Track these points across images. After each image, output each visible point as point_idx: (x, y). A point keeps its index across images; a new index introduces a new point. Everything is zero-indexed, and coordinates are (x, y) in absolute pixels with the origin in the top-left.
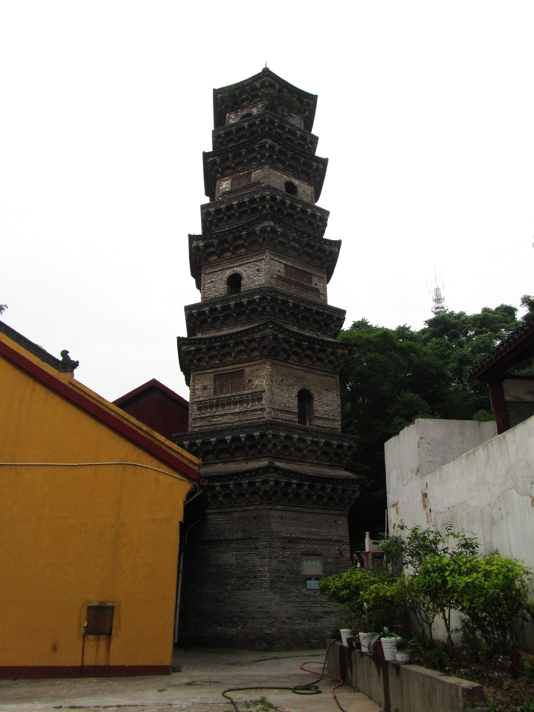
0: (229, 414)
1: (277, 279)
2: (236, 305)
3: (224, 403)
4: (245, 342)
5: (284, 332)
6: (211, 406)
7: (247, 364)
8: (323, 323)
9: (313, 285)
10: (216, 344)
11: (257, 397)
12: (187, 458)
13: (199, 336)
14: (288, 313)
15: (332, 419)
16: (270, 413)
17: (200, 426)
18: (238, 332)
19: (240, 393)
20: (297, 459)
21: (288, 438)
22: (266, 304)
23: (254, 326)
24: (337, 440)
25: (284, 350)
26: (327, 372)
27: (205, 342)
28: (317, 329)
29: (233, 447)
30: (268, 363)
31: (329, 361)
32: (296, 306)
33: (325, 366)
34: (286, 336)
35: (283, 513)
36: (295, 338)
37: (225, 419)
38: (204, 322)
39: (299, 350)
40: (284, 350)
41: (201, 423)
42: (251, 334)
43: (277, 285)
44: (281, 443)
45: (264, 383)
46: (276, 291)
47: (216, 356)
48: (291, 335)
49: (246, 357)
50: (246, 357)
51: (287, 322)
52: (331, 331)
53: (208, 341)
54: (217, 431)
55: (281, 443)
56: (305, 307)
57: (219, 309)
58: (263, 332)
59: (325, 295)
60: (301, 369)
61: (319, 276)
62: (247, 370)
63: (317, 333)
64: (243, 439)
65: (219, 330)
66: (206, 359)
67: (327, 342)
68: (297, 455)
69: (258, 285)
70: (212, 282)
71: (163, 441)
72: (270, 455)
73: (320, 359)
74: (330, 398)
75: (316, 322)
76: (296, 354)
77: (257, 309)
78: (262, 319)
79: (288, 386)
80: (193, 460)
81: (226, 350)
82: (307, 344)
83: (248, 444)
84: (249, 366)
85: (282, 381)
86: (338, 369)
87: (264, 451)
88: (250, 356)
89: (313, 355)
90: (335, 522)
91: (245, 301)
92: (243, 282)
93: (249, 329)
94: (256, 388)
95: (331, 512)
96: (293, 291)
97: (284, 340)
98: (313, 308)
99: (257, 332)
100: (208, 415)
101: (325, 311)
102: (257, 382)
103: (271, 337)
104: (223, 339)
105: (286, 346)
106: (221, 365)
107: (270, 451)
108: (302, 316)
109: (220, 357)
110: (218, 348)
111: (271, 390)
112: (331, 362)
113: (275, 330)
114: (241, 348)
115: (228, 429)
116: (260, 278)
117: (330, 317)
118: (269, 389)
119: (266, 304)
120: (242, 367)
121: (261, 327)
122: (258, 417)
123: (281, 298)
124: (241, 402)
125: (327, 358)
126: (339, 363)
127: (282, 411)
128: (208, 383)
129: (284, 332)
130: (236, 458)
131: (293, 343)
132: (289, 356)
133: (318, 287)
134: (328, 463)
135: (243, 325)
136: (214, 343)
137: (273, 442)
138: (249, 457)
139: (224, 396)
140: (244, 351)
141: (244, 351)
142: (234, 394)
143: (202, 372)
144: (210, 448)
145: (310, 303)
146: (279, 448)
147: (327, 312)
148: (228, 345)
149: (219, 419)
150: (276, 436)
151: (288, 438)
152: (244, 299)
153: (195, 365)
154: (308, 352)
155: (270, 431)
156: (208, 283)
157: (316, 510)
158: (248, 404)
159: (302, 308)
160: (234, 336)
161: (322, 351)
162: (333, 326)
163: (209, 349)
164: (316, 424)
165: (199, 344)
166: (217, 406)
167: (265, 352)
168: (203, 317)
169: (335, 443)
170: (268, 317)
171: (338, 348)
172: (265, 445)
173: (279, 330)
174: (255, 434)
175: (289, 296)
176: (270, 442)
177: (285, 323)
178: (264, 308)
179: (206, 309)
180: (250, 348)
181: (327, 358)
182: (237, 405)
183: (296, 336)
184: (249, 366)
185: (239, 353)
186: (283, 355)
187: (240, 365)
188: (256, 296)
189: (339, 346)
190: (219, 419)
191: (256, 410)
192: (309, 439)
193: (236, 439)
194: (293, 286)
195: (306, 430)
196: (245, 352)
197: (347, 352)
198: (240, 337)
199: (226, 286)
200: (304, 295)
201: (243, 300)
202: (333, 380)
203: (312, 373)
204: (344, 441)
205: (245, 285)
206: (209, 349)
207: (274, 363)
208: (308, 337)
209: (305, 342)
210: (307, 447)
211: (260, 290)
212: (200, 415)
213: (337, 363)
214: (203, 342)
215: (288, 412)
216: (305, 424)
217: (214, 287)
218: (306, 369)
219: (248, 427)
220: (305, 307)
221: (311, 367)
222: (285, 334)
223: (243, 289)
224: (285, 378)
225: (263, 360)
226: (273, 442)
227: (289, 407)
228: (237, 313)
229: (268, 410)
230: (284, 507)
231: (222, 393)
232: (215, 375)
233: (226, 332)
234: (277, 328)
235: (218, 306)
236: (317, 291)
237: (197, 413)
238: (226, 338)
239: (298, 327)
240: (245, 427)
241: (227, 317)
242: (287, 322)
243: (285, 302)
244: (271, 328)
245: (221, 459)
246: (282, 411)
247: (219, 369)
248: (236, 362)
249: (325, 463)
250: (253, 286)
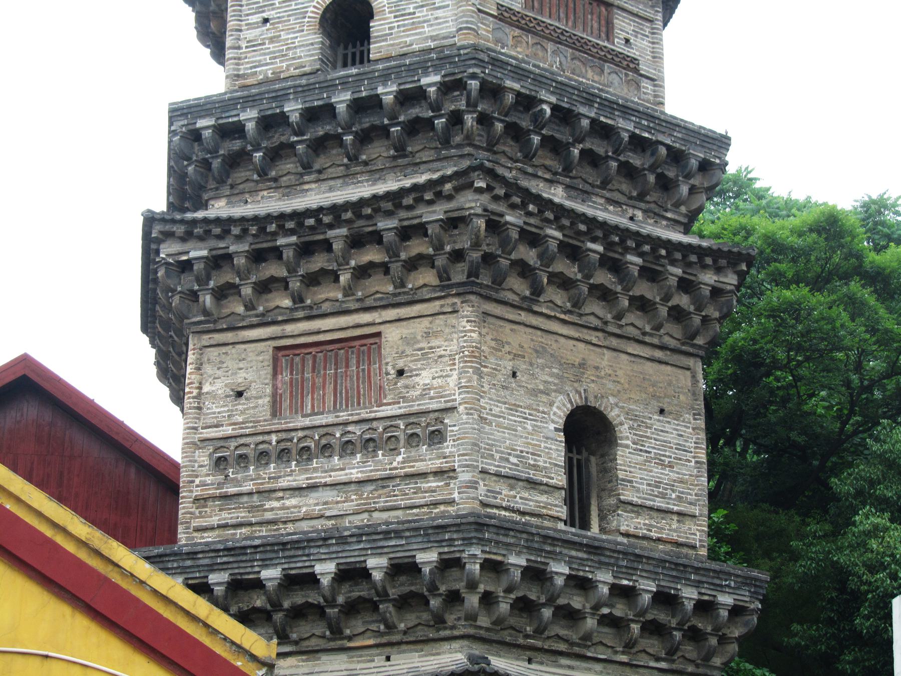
0: (325, 485)
1: (500, 18)
2: (359, 106)
3: (308, 448)
4: (388, 237)
5: (524, 205)
6: (263, 457)
7: (391, 314)
8: (652, 178)
9: (618, 45)
10: (281, 241)
11: (428, 429)
12: (225, 639)
13: (219, 208)
14: (536, 139)
15: (680, 514)
16: (473, 485)
17: (220, 527)
18: (362, 203)
19: (365, 414)
20: (562, 647)
21: (536, 574)
22: (462, 105)
23: (422, 179)
24: (697, 584)
25: (523, 269)
26: (662, 348)
27: (245, 231)
28: (631, 198)
29: (341, 599)
30: (467, 310)
31: (671, 309)
32: (563, 115)
33: (657, 328)
34: (532, 221)
36: (561, 228)
37: (310, 503)
38: (236, 160)
39: (572, 271)
40: (523, 269)
41: (224, 514)
42: (410, 208)
43: (497, 41)
44: (509, 590)
45: (452, 381)
46: (497, 63)
47: (284, 283)
48: (549, 215)
49: (390, 288)
50: (390, 288)
51: (530, 170)
52: (677, 205)
53: (253, 230)
54: (284, 544)
55: (509, 590)
56: (594, 122)
57: (294, 118)
58: (452, 205)
59: (656, 81)
60: (576, 335)
61: (636, 15)
62: (392, 335)
63: (630, 212)
64: (377, 576)
65: (290, 190)
66: (247, 291)
67: (668, 244)
68: (563, 632)
69: (433, 38)
70: (266, 21)
71: (143, 577)
72: (471, 631)
73: (642, 305)
74: (672, 438)
75: (629, 172)
76: (564, 283)
77: (429, 122)
78: (446, 158)
79: (534, 393)
80: (246, 646)
81: (319, 262)
82: (600, 248)
83: (393, 593)
84: (399, 320)
85: (514, 375)
86: (700, 341)
87: (450, 619)
88: (403, 285)
89: (619, 288)
91: (387, 92)
92: (377, 26)
93: (402, 192)
94: (422, 396)
96: (552, 60)
97: (523, 232)
98: (621, 123)
99: (430, 203)
100: (248, 487)
101: (661, 138)
102: (425, 377)
103: (481, 223)
104: (311, 222)
105: (530, 256)
106: (300, 314)
107: (471, 617)
108: (582, 152)
109: (295, 284)
110: (288, 254)
111: (474, 408)
112: (677, 315)
113: (496, 198)
114: (372, 255)
115: (325, 539)
116: (439, 13)
117: (677, 157)
118: (472, 404)
119: (462, 105)
120: (372, 324)
121: (448, 186)
122: (428, 498)
123: (516, 86)
124: (369, 445)
125: (666, 298)
126: (705, 320)
127: (512, 479)
128: (250, 377)
129: (524, 205)
130: (350, 638)
131: (553, 245)
132: (537, 291)
133: (633, 52)
134: (663, 665)
135: (377, 174)
136: (274, 234)
137: (482, 588)
138: (396, 638)
139: (307, 422)
140: (385, 268)
141: (385, 268)
142: (344, 416)
143: (229, 337)
144: (258, 603)
145: (610, 106)
146: (504, 607)
147: (668, 141)
148: (327, 246)
149: (288, 503)
150: (493, 567)
151: (536, 574)
152: (385, 85)
153: (205, 312)
154: (603, 278)
155: (476, 550)
156: (250, 26)
158: (395, 451)
159: (585, 123)
160: (349, 215)
161: (650, 274)
162: (684, 189)
163: (258, 257)
164: (623, 528)
165: (220, 237)
166: (283, 455)
167: (459, 274)
168: (236, 145)
169: (689, 594)
170: (467, 150)
171: (704, 267)
172: (454, 598)
173: (507, 196)
174: (421, 557)
175: (540, 80)
176: (472, 586)
177: (526, 173)
178: (456, 119)
179: (249, 117)
180: (403, 256)
181: (666, 298)
182: (353, 454)
183: (566, 222)
184: (399, 320)
185: (363, 272)
186: (518, 286)
187: (366, 318)
188: (426, 74)
189: (709, 261)
190: (288, 503)
191: (423, 475)
192: (604, 578)
193: (352, 574)
194: (550, 46)
195: (594, 549)
196: (387, 271)
197: (731, 279)
198: (369, 217)
199: (317, 38)
200: (589, 78)
201: (380, 90)
202: (684, 378)
203: (615, 350)
204: (721, 588)
205: (384, 38)
206: (258, 257)
207: (485, 314)
208: (604, 225)
209: (594, 240)
210: (596, 607)
211: (439, 56)
212: (220, 485)
213: (697, 320)
214: (236, 231)
215: (532, 484)
216: (585, 525)
217: (272, 40)
218: (593, 337)
219: (398, 534)
220: (594, 122)
221: (611, 328)
222: (529, 214)
223: (377, 49)
224: (522, 366)
225: (450, 301)
226: (482, 588)
227: (535, 467)
228: (356, 134)
229: (465, 476)
231: (297, 409)
232: (278, 349)
233: (315, 197)
234: (501, 192)
235: (293, 108)
236: (629, 65)
237: (209, 479)
238: (319, 221)
239: (568, 187)
240: (387, 535)
241: (319, 146)
242: (530, 170)
243: (527, 102)
244: (480, 191)
245: (296, 643)
246: (512, 479)
247: (290, 328)
248: (353, 306)
249: (652, 664)
250: (416, 39)
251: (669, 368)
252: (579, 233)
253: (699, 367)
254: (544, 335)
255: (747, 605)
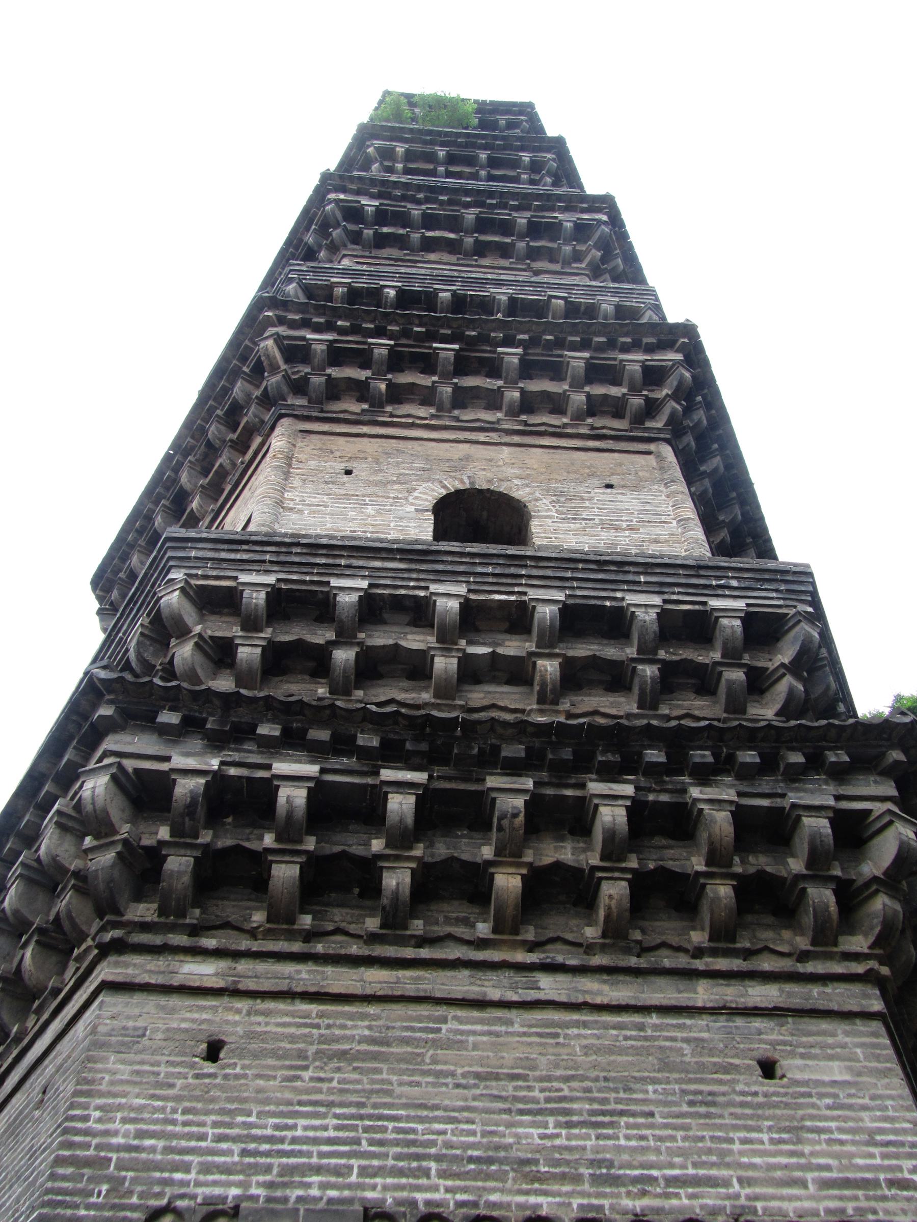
24: (658, 588)
35: (230, 1019)
90: (768, 1069)
95: (703, 993)
157: (550, 986)
230: (243, 966)
251: (616, 455)
252: (419, 337)
253: (667, 451)
254: (401, 442)
255: (784, 611)
